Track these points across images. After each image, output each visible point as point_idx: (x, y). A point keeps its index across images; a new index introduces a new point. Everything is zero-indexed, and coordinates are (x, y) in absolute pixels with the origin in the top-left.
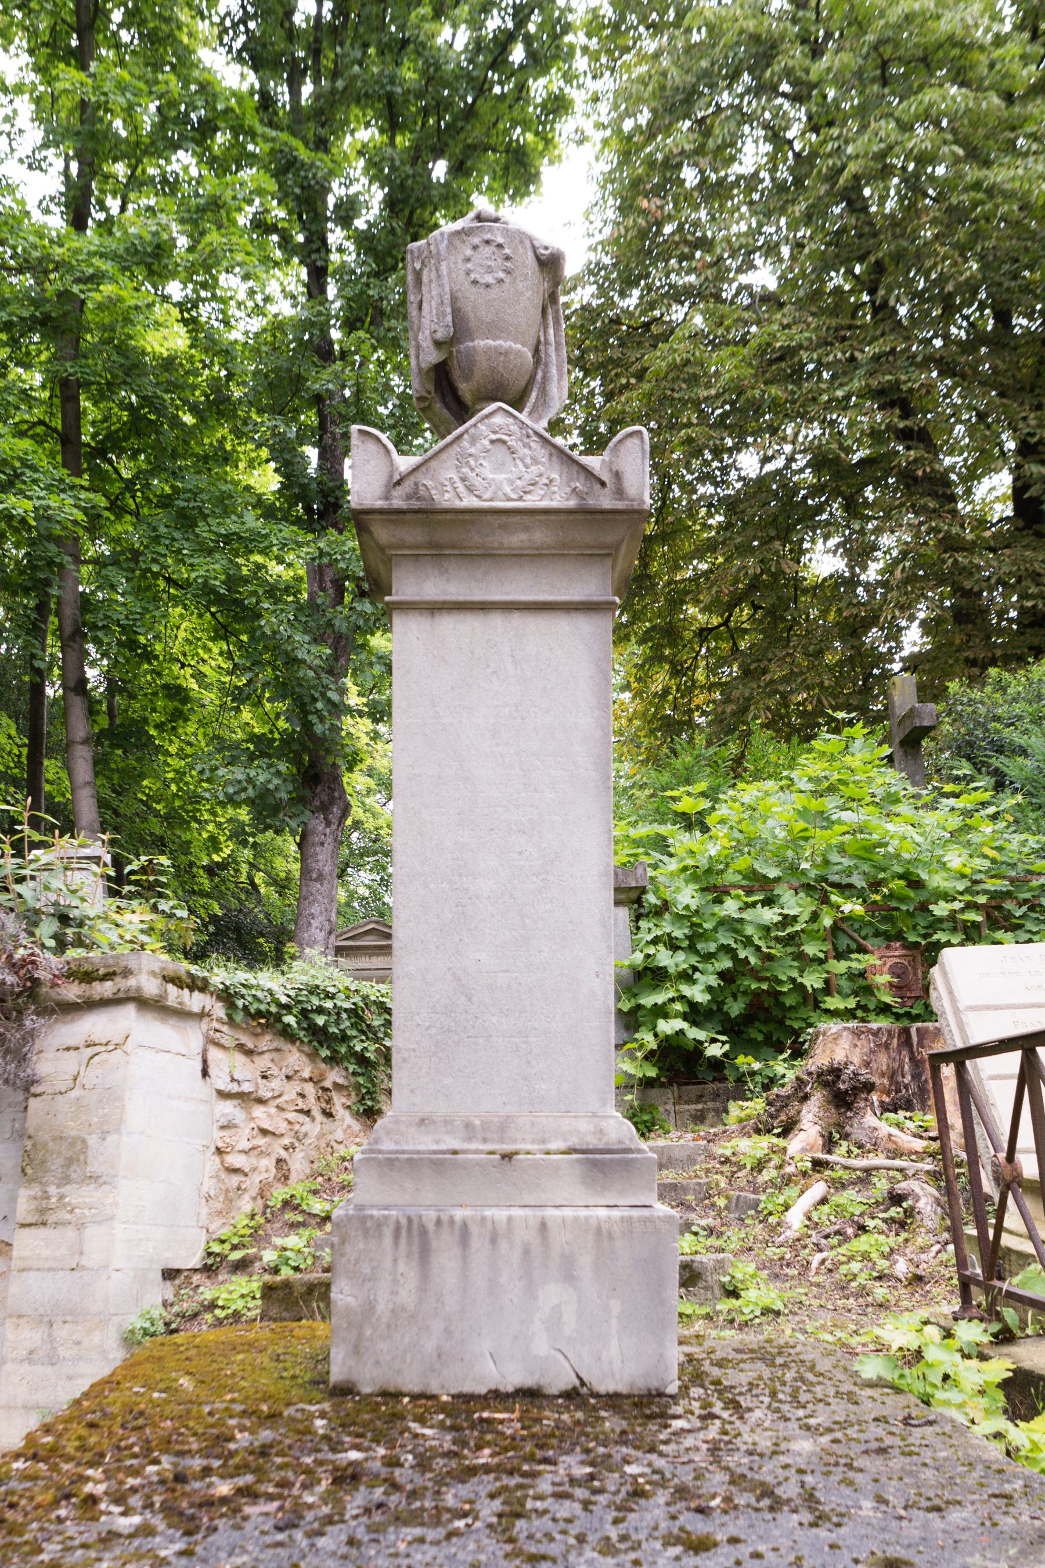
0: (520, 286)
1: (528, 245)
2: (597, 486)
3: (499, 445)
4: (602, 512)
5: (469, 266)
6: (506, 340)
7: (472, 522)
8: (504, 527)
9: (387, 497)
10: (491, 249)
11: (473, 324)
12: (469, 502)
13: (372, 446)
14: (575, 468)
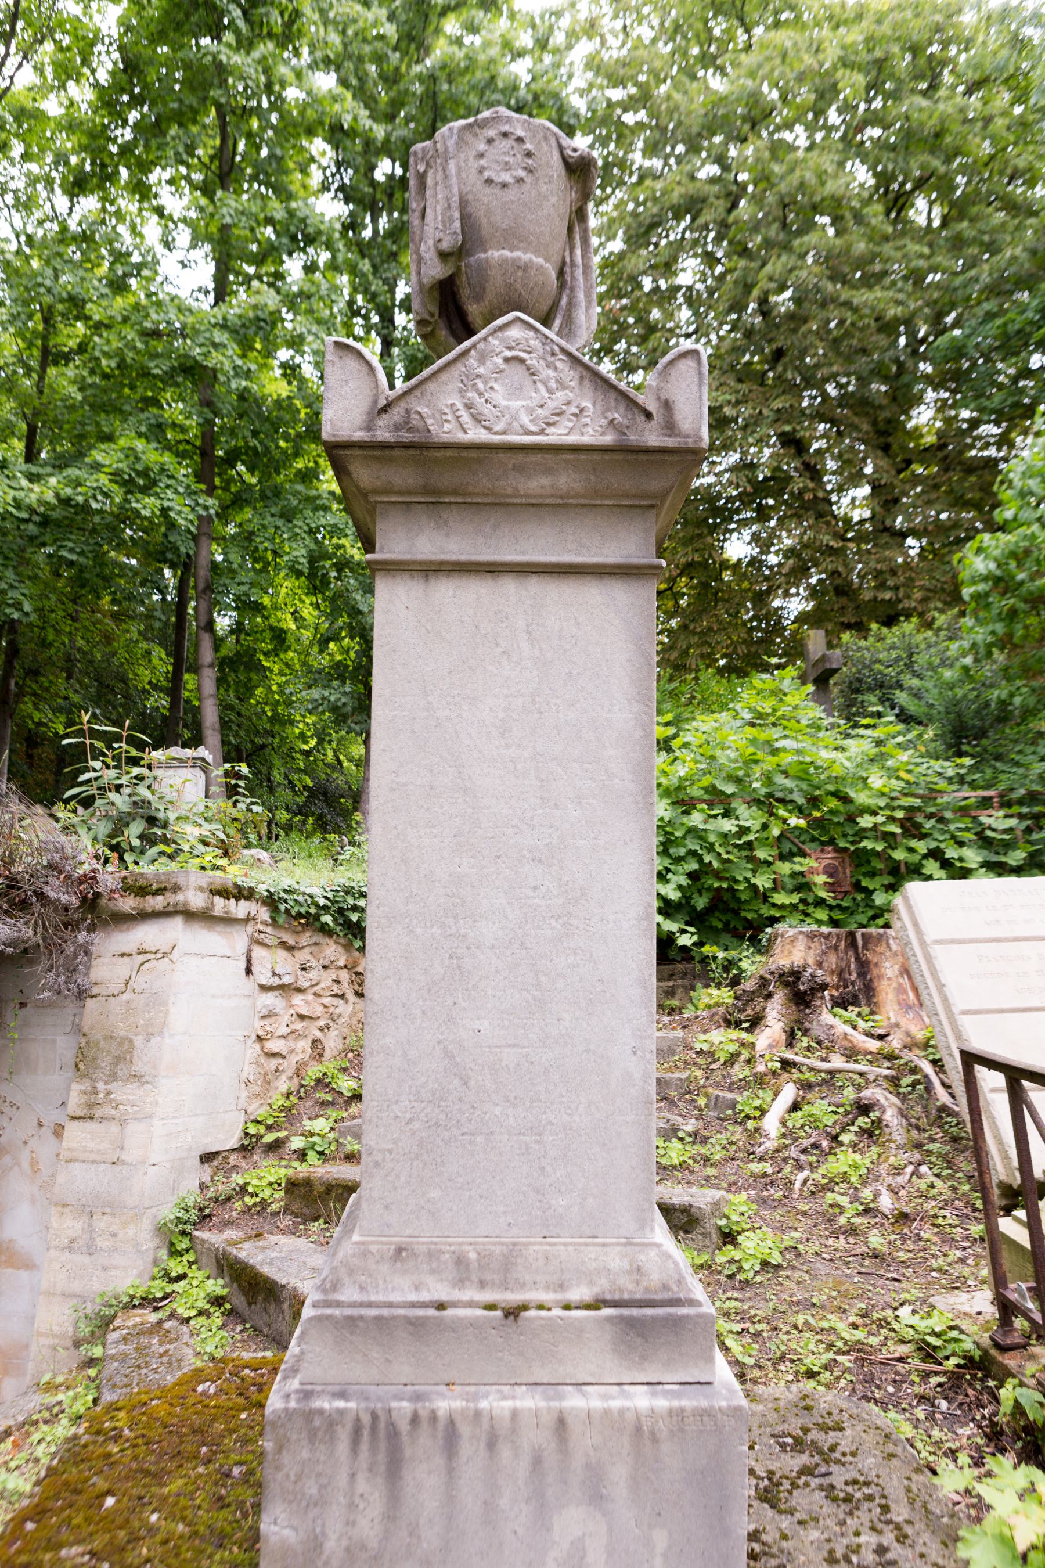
6: (526, 251)
7: (479, 461)
8: (519, 469)
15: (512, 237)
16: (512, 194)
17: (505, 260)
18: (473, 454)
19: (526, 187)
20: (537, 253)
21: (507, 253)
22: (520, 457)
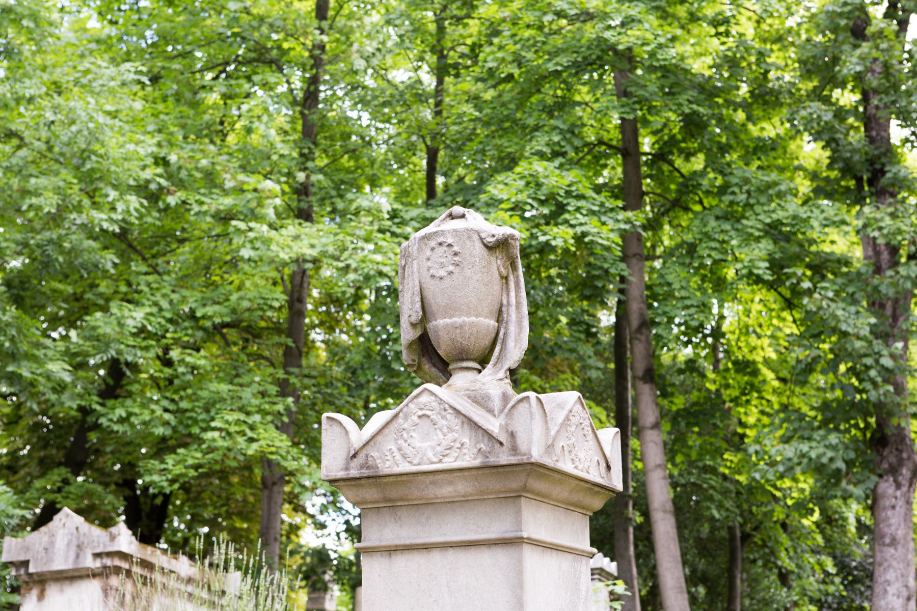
0: (468, 272)
1: (476, 237)
2: (497, 445)
3: (425, 419)
4: (502, 466)
5: (429, 264)
6: (460, 316)
7: (410, 481)
8: (434, 483)
9: (347, 469)
10: (444, 248)
11: (434, 308)
12: (405, 467)
13: (336, 429)
14: (480, 432)
15: (450, 310)
16: (446, 283)
17: (447, 325)
18: (404, 478)
19: (454, 276)
20: (468, 315)
21: (448, 321)
22: (431, 478)
